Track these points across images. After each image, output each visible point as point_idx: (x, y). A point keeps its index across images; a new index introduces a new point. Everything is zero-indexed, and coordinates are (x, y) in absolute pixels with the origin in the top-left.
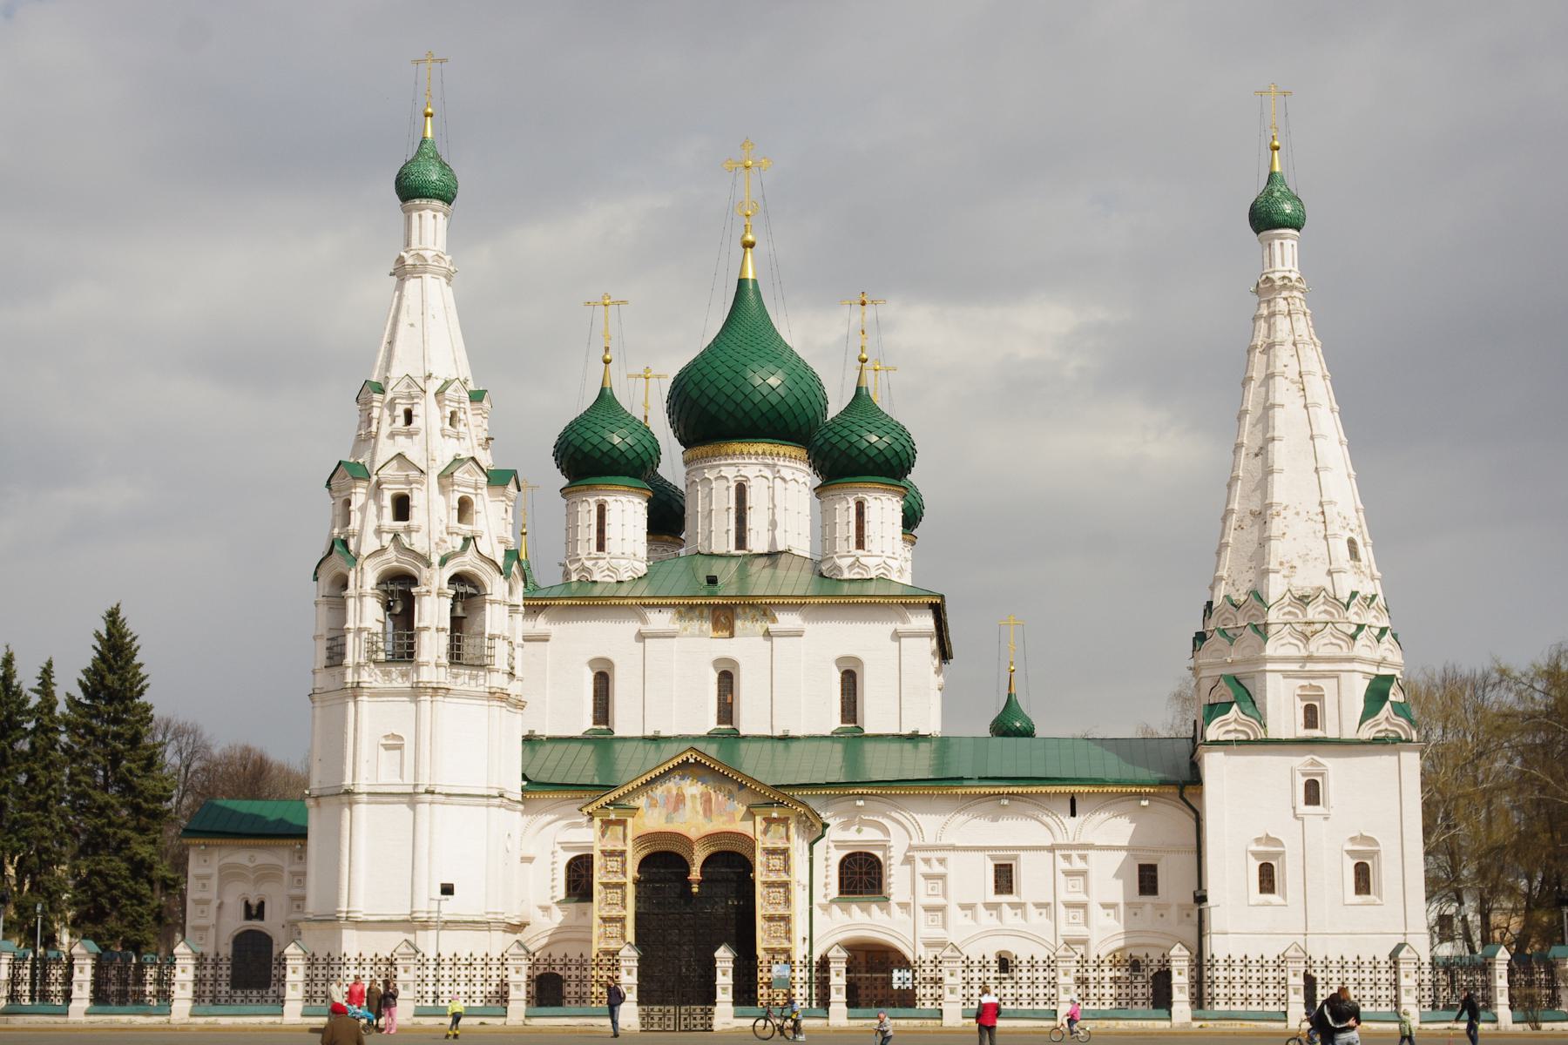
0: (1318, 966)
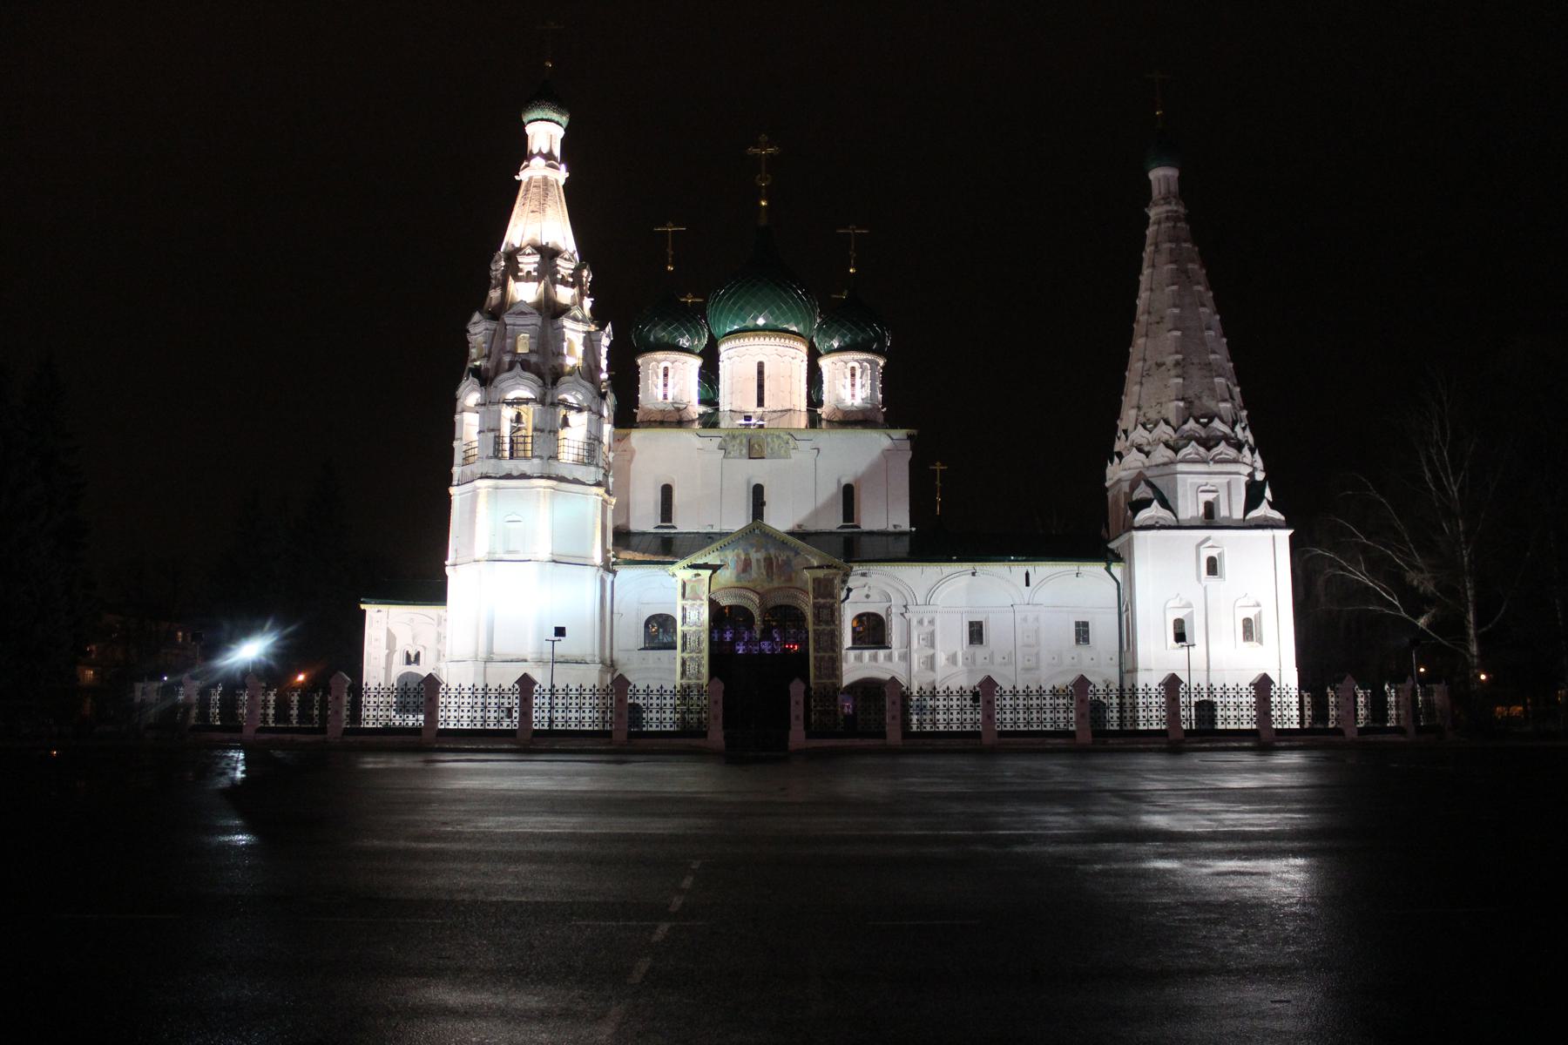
0: (1219, 693)
